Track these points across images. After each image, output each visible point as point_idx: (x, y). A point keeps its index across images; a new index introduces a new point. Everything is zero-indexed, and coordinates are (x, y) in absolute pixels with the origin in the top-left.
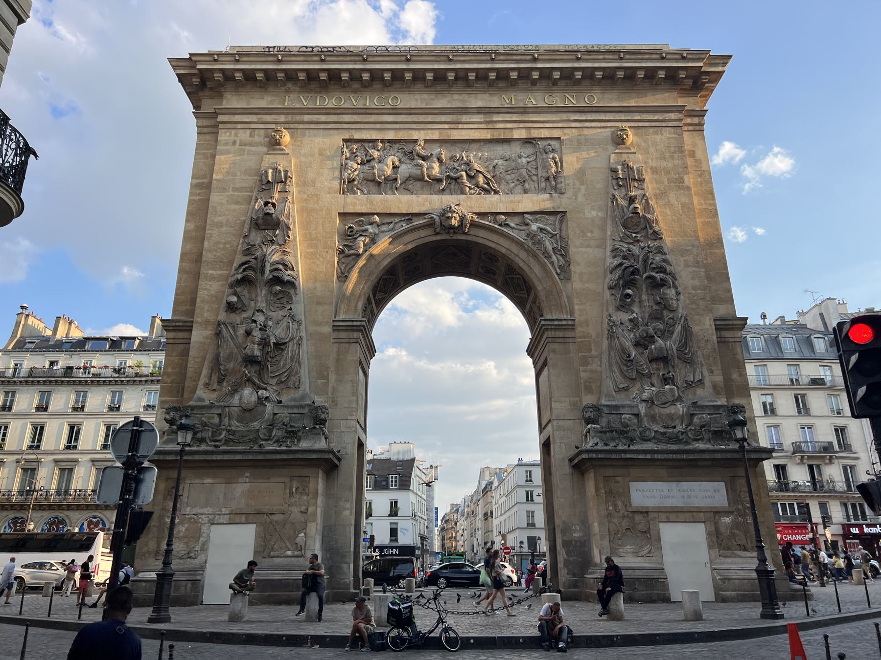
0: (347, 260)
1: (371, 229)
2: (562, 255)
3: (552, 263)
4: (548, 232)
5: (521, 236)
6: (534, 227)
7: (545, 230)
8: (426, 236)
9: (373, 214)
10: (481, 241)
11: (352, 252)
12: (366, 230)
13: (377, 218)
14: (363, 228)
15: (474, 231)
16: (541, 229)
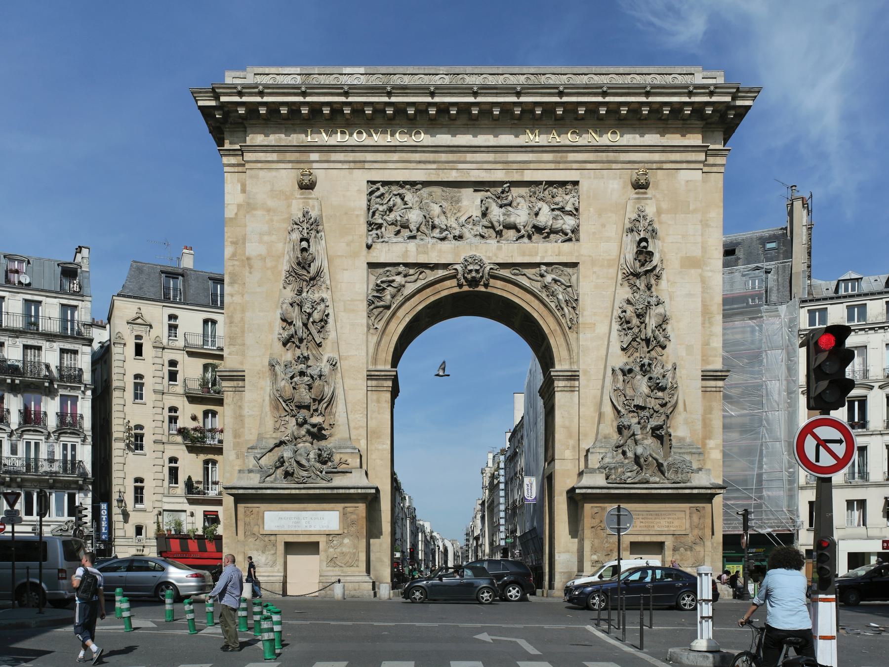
0: (376, 312)
1: (399, 279)
2: (574, 308)
3: (564, 315)
4: (562, 284)
5: (536, 287)
6: (549, 278)
7: (559, 281)
8: (449, 288)
9: (398, 264)
10: (499, 293)
11: (382, 303)
12: (393, 281)
13: (401, 269)
14: (391, 278)
15: (492, 282)
16: (555, 281)
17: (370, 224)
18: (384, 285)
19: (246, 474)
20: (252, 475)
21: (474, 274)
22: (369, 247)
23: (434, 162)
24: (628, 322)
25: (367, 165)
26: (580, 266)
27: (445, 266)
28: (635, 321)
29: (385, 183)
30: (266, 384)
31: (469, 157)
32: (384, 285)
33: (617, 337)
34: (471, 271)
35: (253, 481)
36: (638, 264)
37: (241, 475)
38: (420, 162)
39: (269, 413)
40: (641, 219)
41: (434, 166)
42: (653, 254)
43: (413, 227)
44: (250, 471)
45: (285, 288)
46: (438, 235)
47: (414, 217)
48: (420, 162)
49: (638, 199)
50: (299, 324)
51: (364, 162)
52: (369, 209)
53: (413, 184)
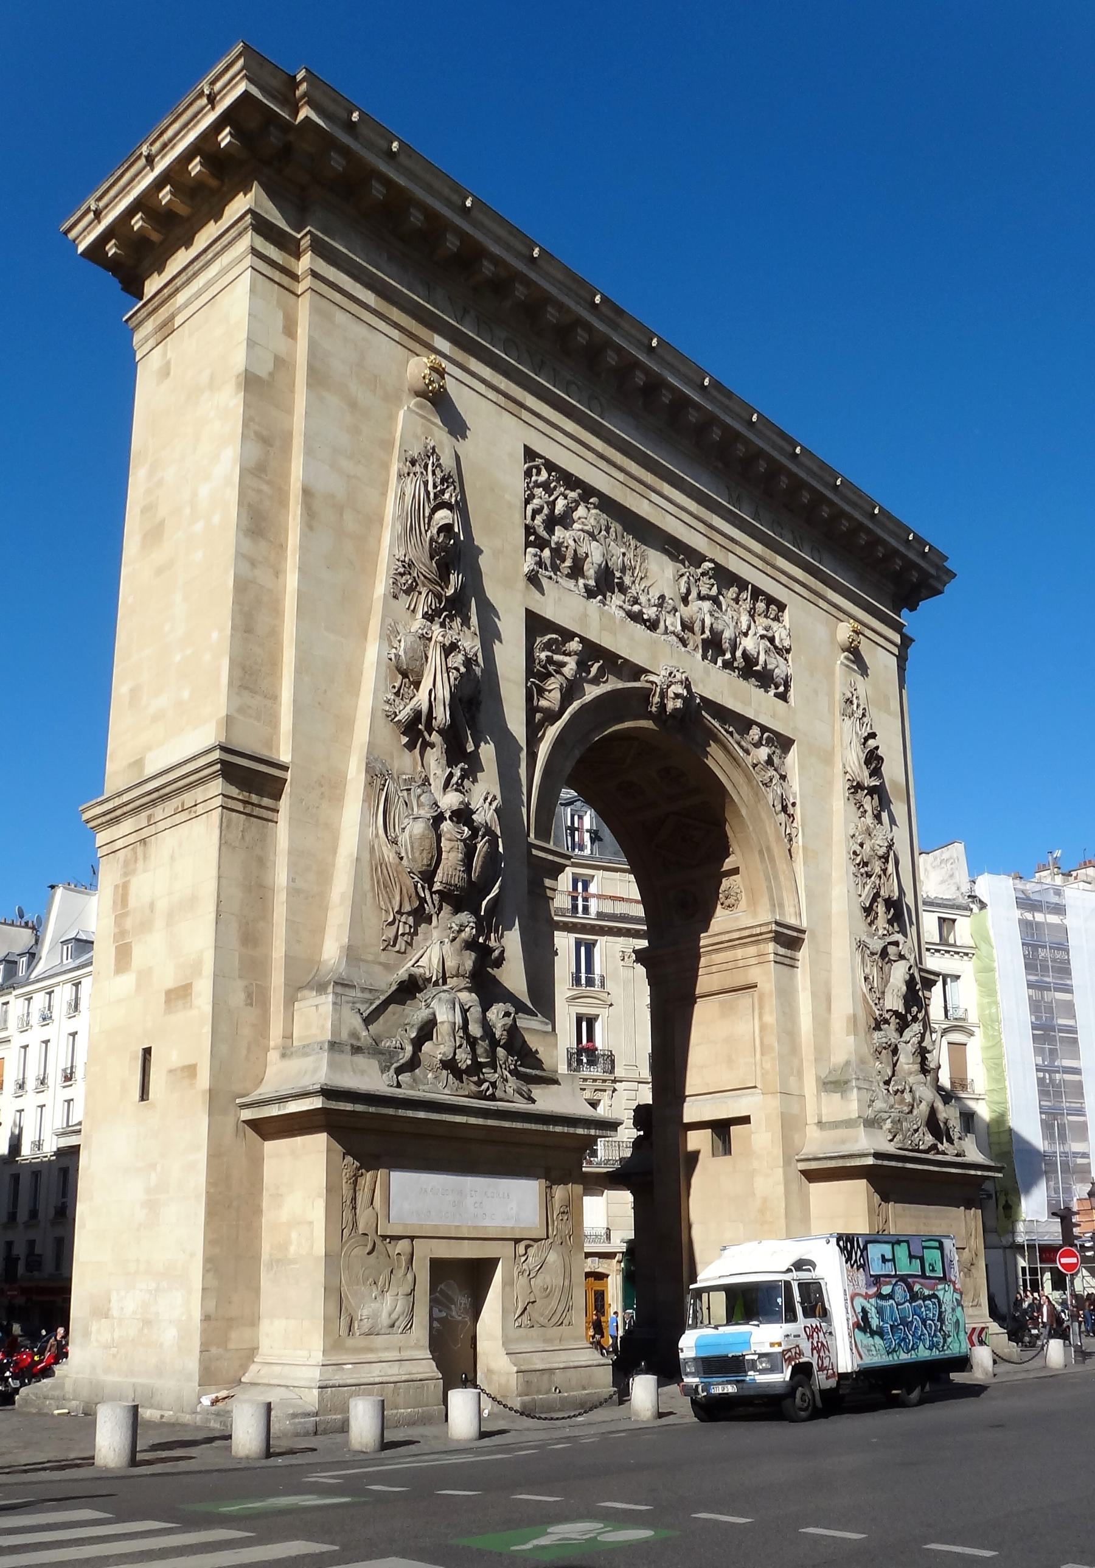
5: (749, 760)
11: (543, 703)
17: (529, 530)
18: (551, 668)
19: (347, 1058)
20: (361, 1060)
21: (679, 704)
22: (533, 579)
23: (621, 469)
24: (866, 864)
25: (525, 415)
26: (794, 748)
27: (638, 672)
28: (877, 867)
29: (550, 466)
30: (352, 818)
31: (667, 489)
32: (551, 668)
33: (854, 885)
34: (677, 696)
35: (371, 1079)
36: (866, 773)
37: (338, 1057)
38: (602, 457)
39: (370, 895)
40: (855, 701)
41: (621, 476)
42: (882, 759)
43: (590, 570)
44: (357, 1050)
45: (395, 597)
46: (627, 607)
47: (595, 554)
48: (602, 457)
49: (847, 666)
50: (443, 693)
51: (522, 405)
52: (527, 502)
53: (588, 492)
